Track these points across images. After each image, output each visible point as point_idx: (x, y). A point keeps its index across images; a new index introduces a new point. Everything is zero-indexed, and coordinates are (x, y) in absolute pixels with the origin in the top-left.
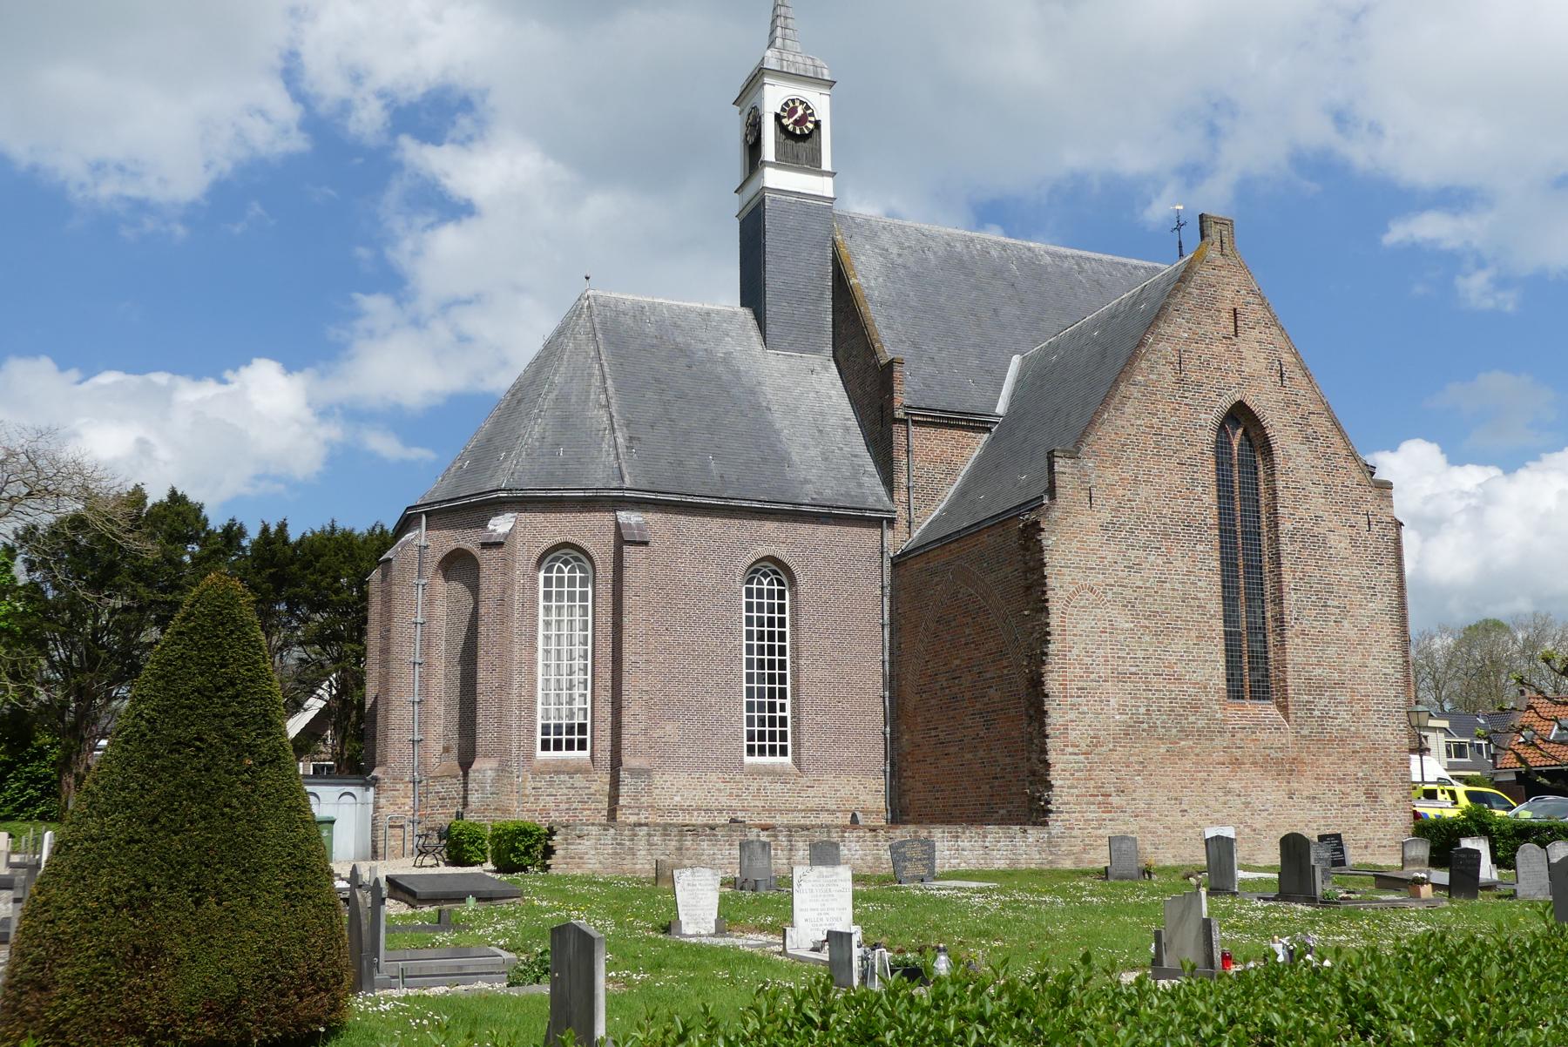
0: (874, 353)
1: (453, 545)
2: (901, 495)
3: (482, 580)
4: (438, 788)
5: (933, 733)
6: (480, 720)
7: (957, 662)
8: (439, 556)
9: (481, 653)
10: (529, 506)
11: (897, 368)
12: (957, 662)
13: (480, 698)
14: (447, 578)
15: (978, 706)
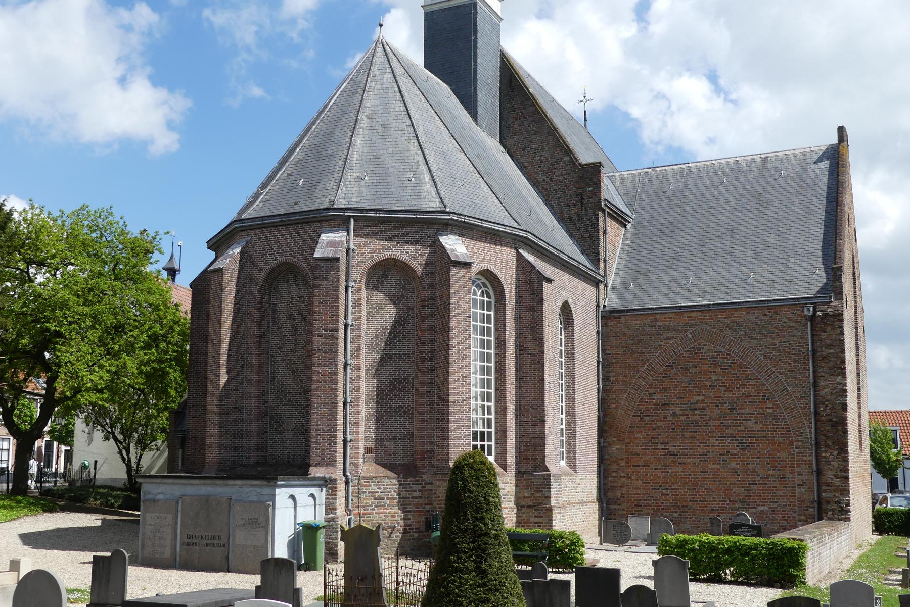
0: (569, 152)
1: (386, 254)
2: (601, 265)
3: (452, 296)
4: (374, 488)
5: (660, 447)
6: (452, 427)
7: (701, 398)
8: (369, 262)
9: (452, 364)
10: (464, 232)
11: (603, 171)
12: (701, 398)
13: (452, 407)
14: (370, 285)
15: (729, 431)
